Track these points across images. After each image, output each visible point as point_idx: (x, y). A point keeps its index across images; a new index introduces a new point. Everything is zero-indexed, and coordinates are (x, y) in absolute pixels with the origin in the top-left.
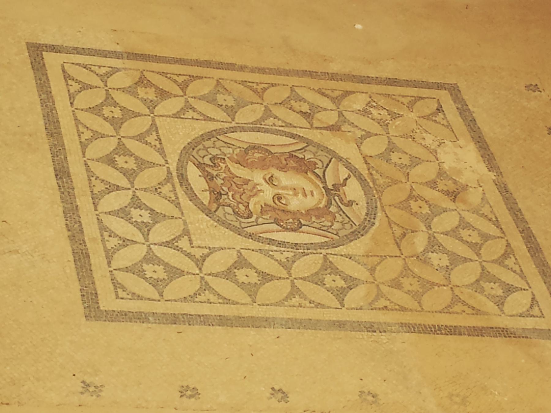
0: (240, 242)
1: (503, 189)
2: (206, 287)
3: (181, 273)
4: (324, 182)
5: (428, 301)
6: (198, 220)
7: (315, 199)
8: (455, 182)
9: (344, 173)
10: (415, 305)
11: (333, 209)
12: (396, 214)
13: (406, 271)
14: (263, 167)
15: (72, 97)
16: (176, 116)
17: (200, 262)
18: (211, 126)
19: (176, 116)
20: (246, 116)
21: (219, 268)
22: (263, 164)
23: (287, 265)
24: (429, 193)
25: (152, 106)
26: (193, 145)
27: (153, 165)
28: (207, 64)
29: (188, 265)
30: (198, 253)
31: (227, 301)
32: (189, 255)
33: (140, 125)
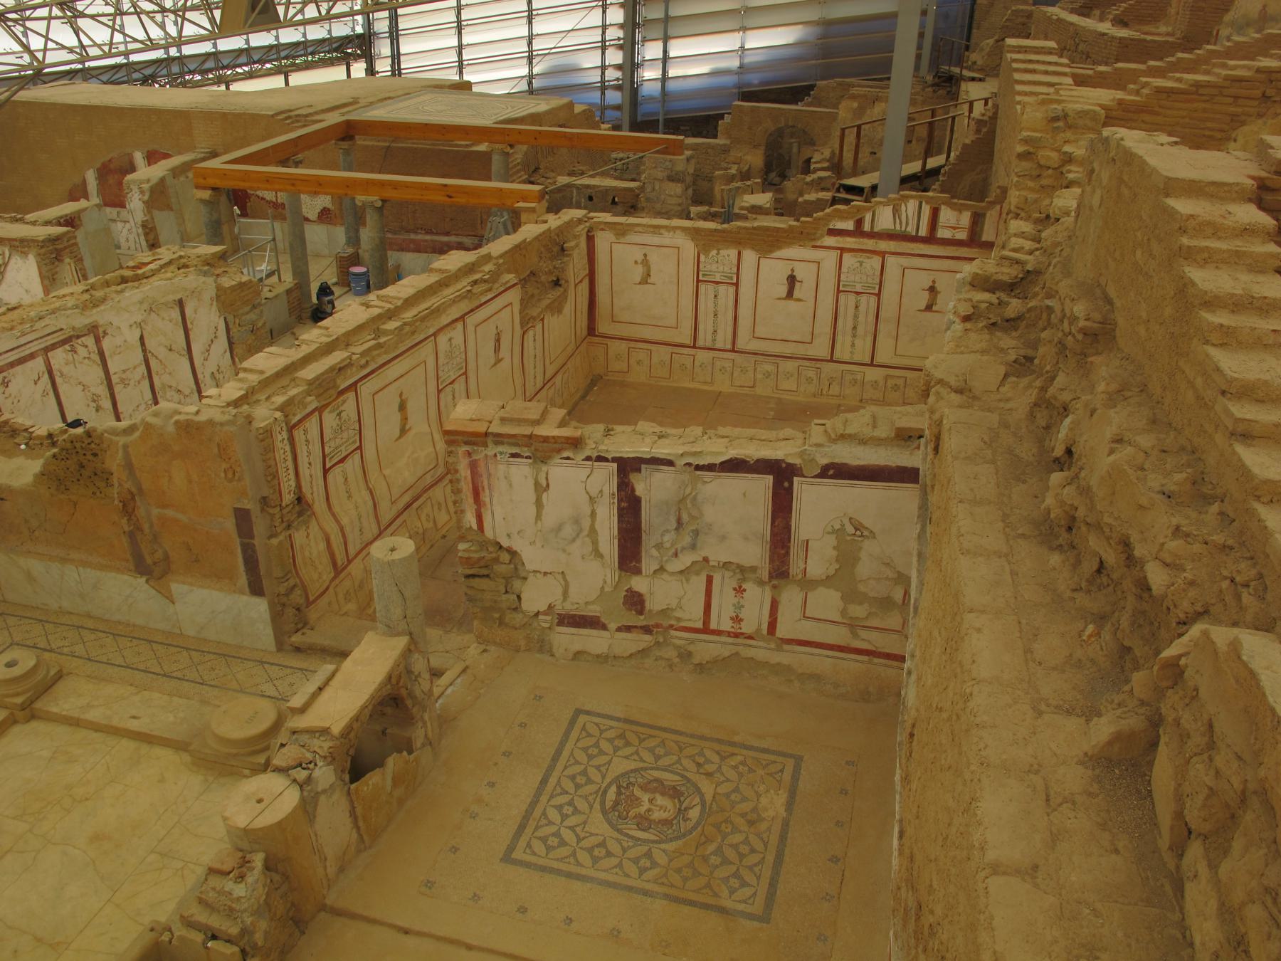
1: (786, 825)
4: (681, 803)
6: (597, 816)
9: (697, 800)
16: (626, 757)
17: (579, 840)
18: (642, 765)
19: (626, 757)
20: (665, 761)
22: (654, 791)
24: (739, 821)
25: (616, 749)
26: (622, 775)
32: (577, 836)
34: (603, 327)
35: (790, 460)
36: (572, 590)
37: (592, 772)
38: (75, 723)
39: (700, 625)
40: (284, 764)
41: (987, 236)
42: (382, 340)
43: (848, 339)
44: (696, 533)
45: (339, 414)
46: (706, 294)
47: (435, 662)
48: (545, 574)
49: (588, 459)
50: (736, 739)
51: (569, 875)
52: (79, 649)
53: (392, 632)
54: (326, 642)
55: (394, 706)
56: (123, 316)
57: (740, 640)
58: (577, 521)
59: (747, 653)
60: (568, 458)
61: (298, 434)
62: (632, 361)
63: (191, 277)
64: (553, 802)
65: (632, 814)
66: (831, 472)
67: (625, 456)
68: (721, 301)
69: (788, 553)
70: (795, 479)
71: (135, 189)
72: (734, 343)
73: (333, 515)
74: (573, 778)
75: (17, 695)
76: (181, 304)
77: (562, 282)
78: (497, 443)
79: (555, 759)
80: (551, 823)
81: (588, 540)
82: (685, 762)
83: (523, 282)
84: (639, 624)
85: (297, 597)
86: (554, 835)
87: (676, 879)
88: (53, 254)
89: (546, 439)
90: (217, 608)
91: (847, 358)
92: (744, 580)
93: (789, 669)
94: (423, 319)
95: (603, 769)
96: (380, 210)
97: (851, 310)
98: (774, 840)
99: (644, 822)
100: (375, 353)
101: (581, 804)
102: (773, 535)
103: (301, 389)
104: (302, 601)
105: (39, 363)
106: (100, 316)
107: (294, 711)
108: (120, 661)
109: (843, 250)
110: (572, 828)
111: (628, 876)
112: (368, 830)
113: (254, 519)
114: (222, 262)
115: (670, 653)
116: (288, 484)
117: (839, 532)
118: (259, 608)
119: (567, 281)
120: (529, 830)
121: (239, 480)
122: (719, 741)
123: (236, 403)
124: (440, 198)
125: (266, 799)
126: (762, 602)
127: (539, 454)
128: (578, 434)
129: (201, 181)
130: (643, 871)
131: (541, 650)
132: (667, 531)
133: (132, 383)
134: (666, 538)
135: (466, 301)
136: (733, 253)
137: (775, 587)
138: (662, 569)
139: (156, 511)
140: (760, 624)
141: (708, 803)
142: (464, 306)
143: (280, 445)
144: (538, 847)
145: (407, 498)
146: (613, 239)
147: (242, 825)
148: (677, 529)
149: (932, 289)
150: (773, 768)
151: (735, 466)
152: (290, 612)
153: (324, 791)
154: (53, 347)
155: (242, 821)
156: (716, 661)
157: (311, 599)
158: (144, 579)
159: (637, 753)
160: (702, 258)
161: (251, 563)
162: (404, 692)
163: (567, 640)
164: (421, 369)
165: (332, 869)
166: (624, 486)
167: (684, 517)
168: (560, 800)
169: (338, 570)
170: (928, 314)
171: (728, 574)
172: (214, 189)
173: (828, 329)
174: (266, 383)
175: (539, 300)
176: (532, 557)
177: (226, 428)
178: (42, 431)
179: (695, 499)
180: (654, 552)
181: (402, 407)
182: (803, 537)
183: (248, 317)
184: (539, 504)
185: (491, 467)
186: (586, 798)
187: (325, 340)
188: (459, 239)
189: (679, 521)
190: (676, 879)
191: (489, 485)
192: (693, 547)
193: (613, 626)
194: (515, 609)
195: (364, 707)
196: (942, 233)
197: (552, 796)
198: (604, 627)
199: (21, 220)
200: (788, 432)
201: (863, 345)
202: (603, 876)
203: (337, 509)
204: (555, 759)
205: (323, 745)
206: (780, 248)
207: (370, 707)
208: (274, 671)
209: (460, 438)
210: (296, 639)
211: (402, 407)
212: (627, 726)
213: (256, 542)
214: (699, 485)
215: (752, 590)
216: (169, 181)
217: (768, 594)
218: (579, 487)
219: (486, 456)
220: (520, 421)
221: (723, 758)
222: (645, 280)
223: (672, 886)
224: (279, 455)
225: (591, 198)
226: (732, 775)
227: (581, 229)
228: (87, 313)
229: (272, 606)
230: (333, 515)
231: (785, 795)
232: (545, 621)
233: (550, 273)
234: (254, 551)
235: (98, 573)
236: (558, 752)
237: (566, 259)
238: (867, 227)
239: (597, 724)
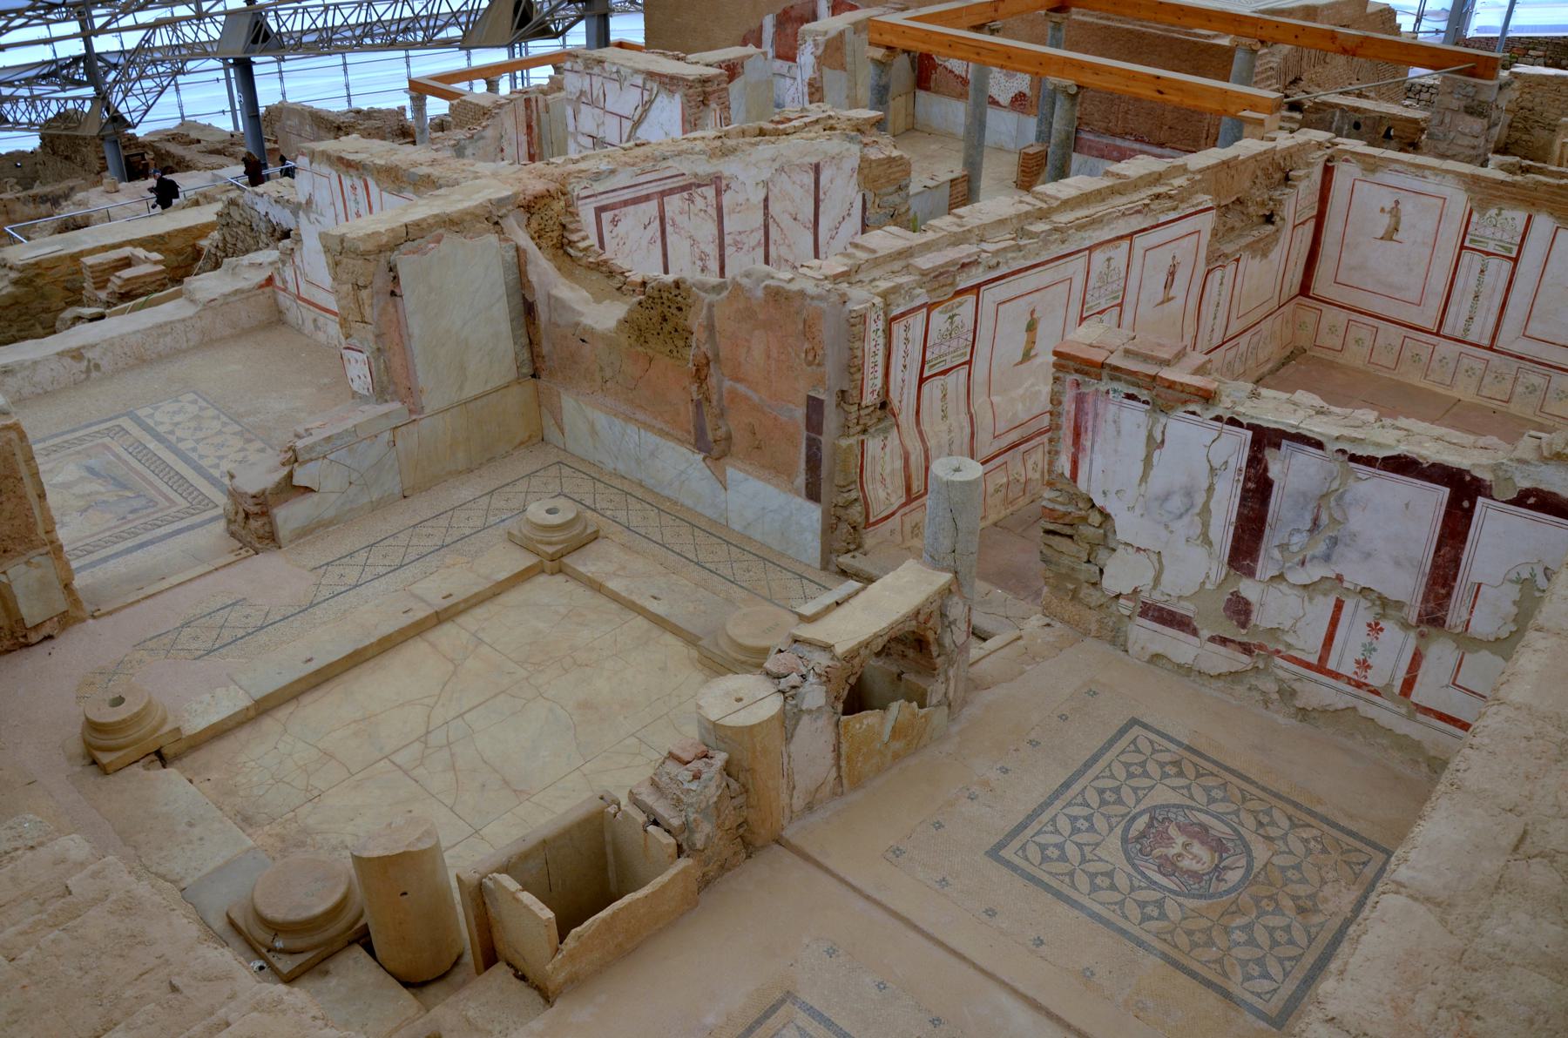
5: (1197, 952)
6: (1114, 841)
8: (1315, 905)
9: (1243, 862)
12: (1245, 898)
16: (1174, 789)
17: (1084, 860)
18: (1189, 802)
19: (1174, 789)
21: (1091, 870)
24: (1287, 903)
25: (1165, 775)
26: (1162, 807)
27: (1124, 804)
32: (1083, 855)
34: (1320, 286)
36: (1165, 578)
37: (1126, 793)
38: (596, 587)
39: (1314, 660)
40: (774, 670)
42: (1022, 243)
44: (1335, 541)
45: (951, 318)
46: (1470, 267)
47: (979, 620)
48: (1139, 549)
49: (1218, 419)
50: (1319, 809)
51: (1058, 895)
52: (621, 516)
53: (936, 563)
55: (914, 647)
56: (748, 171)
57: (1362, 693)
58: (1189, 494)
59: (1365, 710)
60: (1194, 413)
61: (898, 329)
63: (835, 141)
64: (1068, 811)
65: (1157, 852)
67: (1265, 425)
69: (1449, 595)
71: (810, 41)
72: (1494, 338)
73: (920, 433)
74: (1101, 792)
75: (550, 544)
76: (817, 169)
78: (1112, 378)
79: (1088, 765)
80: (1057, 832)
81: (1197, 519)
82: (1243, 815)
83: (1224, 210)
84: (1238, 639)
85: (855, 513)
86: (1056, 845)
87: (1182, 941)
88: (702, 97)
89: (1171, 385)
90: (768, 505)
92: (1384, 616)
93: (1417, 746)
94: (1080, 228)
95: (1141, 793)
96: (1073, 97)
98: (1324, 938)
99: (1168, 866)
100: (1010, 255)
101: (1101, 824)
102: (1435, 566)
103: (912, 278)
104: (860, 519)
105: (654, 204)
106: (728, 167)
107: (804, 619)
110: (1079, 846)
111: (1126, 918)
112: (849, 773)
113: (826, 412)
114: (874, 130)
115: (1270, 686)
116: (873, 382)
118: (812, 514)
119: (1283, 219)
120: (1029, 832)
122: (1296, 805)
123: (836, 278)
124: (1148, 92)
125: (746, 701)
126: (1401, 650)
127: (1160, 402)
128: (1213, 386)
129: (877, 37)
130: (1146, 918)
131: (1113, 642)
132: (1298, 530)
133: (746, 248)
134: (1295, 539)
135: (1139, 217)
137: (1422, 635)
138: (1281, 577)
139: (727, 384)
140: (1392, 678)
141: (1255, 870)
142: (1137, 223)
143: (873, 336)
144: (1033, 852)
145: (1014, 437)
148: (1311, 531)
150: (1354, 858)
151: (1402, 465)
152: (844, 528)
153: (810, 712)
154: (671, 192)
155: (714, 714)
156: (1326, 711)
157: (872, 520)
159: (1188, 788)
161: (813, 463)
162: (931, 636)
163: (1147, 636)
164: (1064, 287)
165: (799, 802)
166: (1256, 461)
168: (1076, 811)
169: (911, 497)
171: (1364, 603)
172: (888, 48)
174: (877, 262)
175: (1241, 236)
176: (1127, 525)
177: (816, 303)
178: (636, 277)
179: (1341, 497)
180: (1276, 554)
181: (1031, 327)
183: (891, 198)
184: (1148, 462)
185: (1101, 406)
186: (1108, 818)
187: (955, 229)
189: (1316, 522)
190: (1182, 941)
192: (1327, 558)
193: (1205, 633)
194: (1094, 584)
195: (877, 636)
197: (1069, 804)
198: (1195, 632)
199: (682, 59)
200: (1492, 440)
202: (1097, 908)
203: (925, 427)
204: (1088, 765)
205: (821, 660)
207: (886, 638)
208: (811, 589)
209: (1071, 363)
210: (845, 560)
211: (1031, 327)
212: (1187, 754)
213: (823, 439)
214: (1351, 481)
215: (1390, 629)
216: (849, 36)
217: (1412, 642)
218: (1202, 454)
219: (1097, 390)
220: (1147, 358)
221: (1293, 826)
223: (1176, 946)
224: (869, 346)
225: (1357, 126)
226: (1298, 848)
228: (714, 161)
229: (825, 514)
230: (920, 433)
232: (1125, 607)
233: (1263, 204)
234: (819, 449)
235: (658, 439)
236: (1094, 759)
237: (1287, 190)
239: (1151, 742)
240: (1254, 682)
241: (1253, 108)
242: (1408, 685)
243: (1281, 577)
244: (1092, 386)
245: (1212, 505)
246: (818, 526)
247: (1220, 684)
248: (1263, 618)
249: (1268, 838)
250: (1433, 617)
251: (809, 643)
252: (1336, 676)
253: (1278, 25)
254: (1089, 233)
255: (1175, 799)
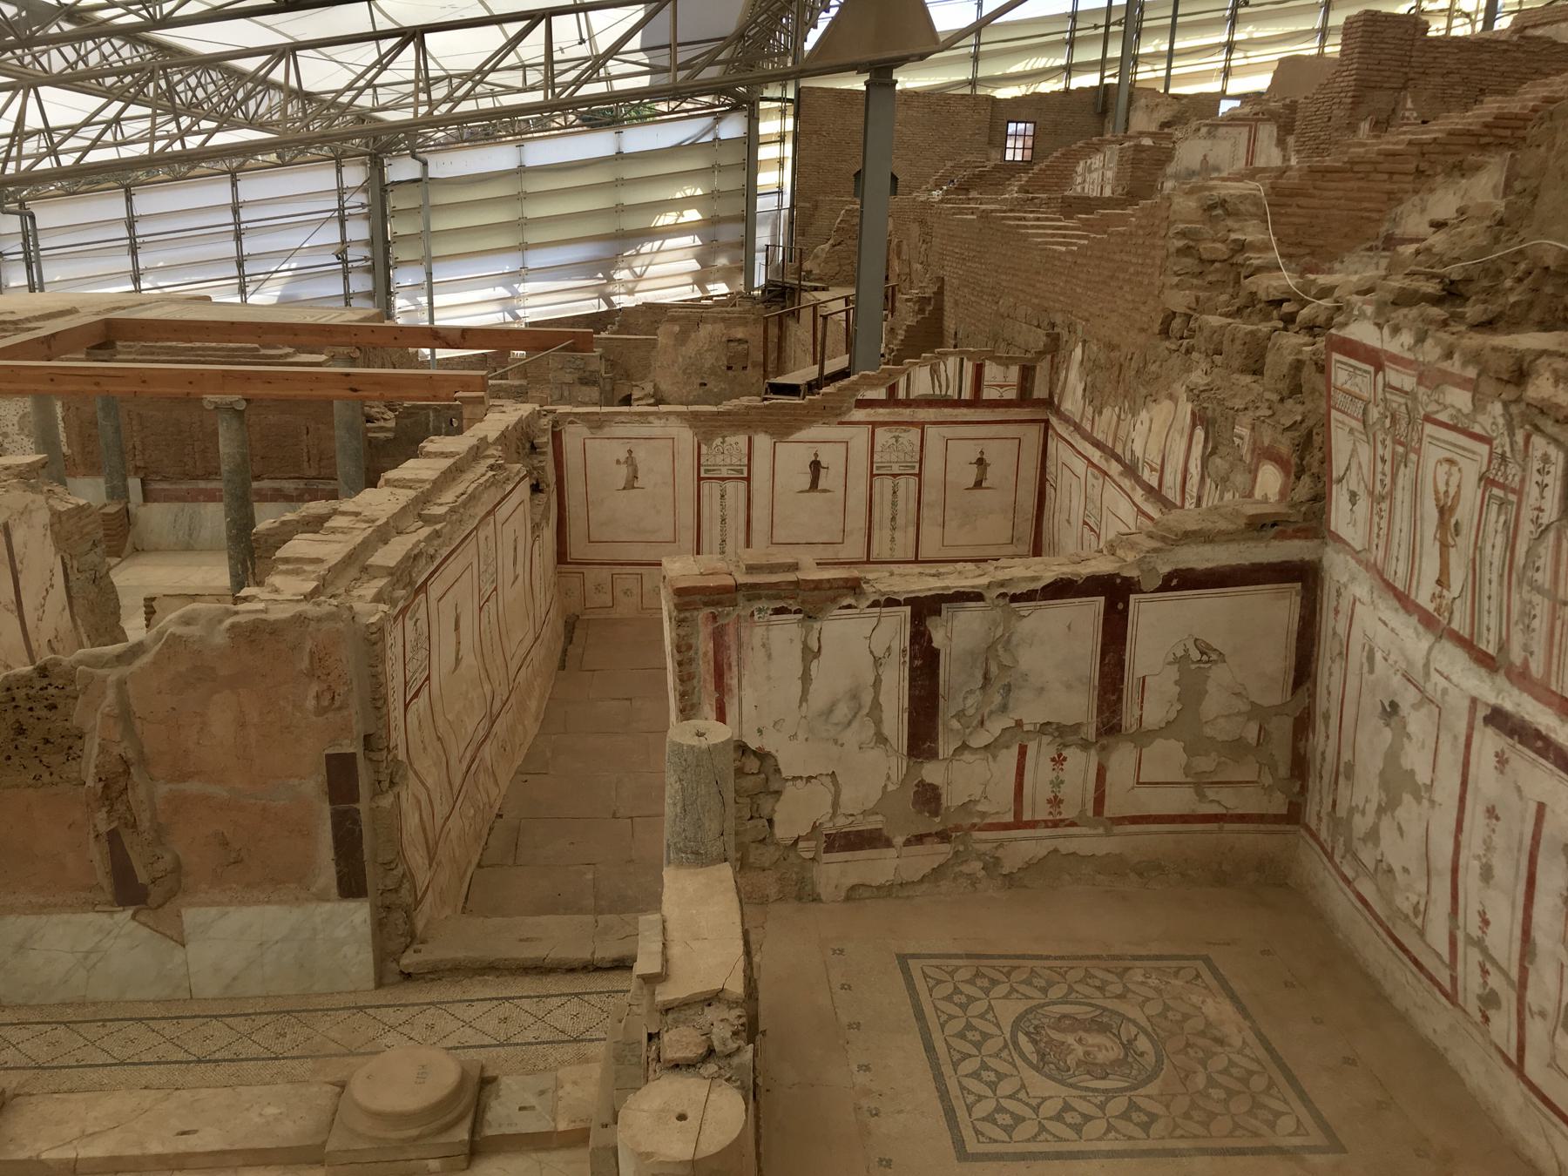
0: (1064, 1091)
2: (1042, 1128)
3: (1024, 1119)
6: (1029, 1075)
7: (1116, 1052)
9: (1134, 1030)
10: (1205, 1133)
11: (1130, 1059)
13: (1194, 1105)
14: (1074, 1031)
15: (930, 990)
16: (1005, 997)
17: (1036, 1109)
19: (1005, 997)
23: (1102, 1107)
25: (987, 992)
27: (992, 1036)
28: (1023, 957)
29: (1028, 1113)
30: (1034, 1103)
31: (1060, 1139)
33: (980, 1006)
35: (1125, 574)
36: (844, 797)
39: (1009, 818)
41: (1040, 392)
43: (887, 533)
44: (1008, 689)
54: (460, 954)
59: (1066, 846)
60: (849, 607)
62: (618, 592)
66: (1174, 582)
67: (922, 595)
68: (729, 501)
69: (1120, 699)
70: (1132, 597)
77: (543, 486)
90: (279, 935)
91: (886, 556)
97: (888, 496)
102: (1102, 675)
104: (410, 900)
108: (102, 1058)
109: (874, 424)
117: (1181, 661)
118: (359, 913)
121: (340, 708)
130: (1145, 1127)
132: (971, 692)
134: (969, 702)
136: (742, 440)
137: (1104, 748)
139: (163, 789)
146: (585, 432)
147: (689, 1157)
148: (983, 687)
149: (980, 462)
151: (1061, 589)
158: (130, 912)
160: (704, 449)
163: (836, 872)
167: (996, 670)
168: (968, 1066)
170: (978, 493)
171: (1046, 739)
173: (862, 523)
176: (791, 757)
177: (325, 626)
179: (1008, 641)
180: (955, 724)
182: (1139, 674)
184: (806, 678)
185: (744, 634)
188: (276, 484)
189: (986, 677)
191: (739, 659)
193: (899, 840)
196: (988, 394)
198: (888, 844)
201: (905, 539)
206: (800, 429)
208: (390, 1015)
209: (697, 597)
210: (409, 960)
211: (457, 628)
215: (1074, 756)
218: (861, 644)
220: (773, 568)
222: (630, 485)
227: (545, 422)
229: (375, 909)
231: (1228, 1001)
234: (356, 822)
238: (901, 395)
240: (957, 869)
241: (466, 387)
242: (1099, 801)
243: (964, 747)
244: (729, 615)
245: (882, 699)
246: (367, 930)
247: (925, 886)
248: (952, 798)
249: (1118, 997)
250: (1110, 726)
251: (686, 1004)
252: (1033, 824)
253: (373, 330)
254: (472, 511)
255: (1022, 1006)
